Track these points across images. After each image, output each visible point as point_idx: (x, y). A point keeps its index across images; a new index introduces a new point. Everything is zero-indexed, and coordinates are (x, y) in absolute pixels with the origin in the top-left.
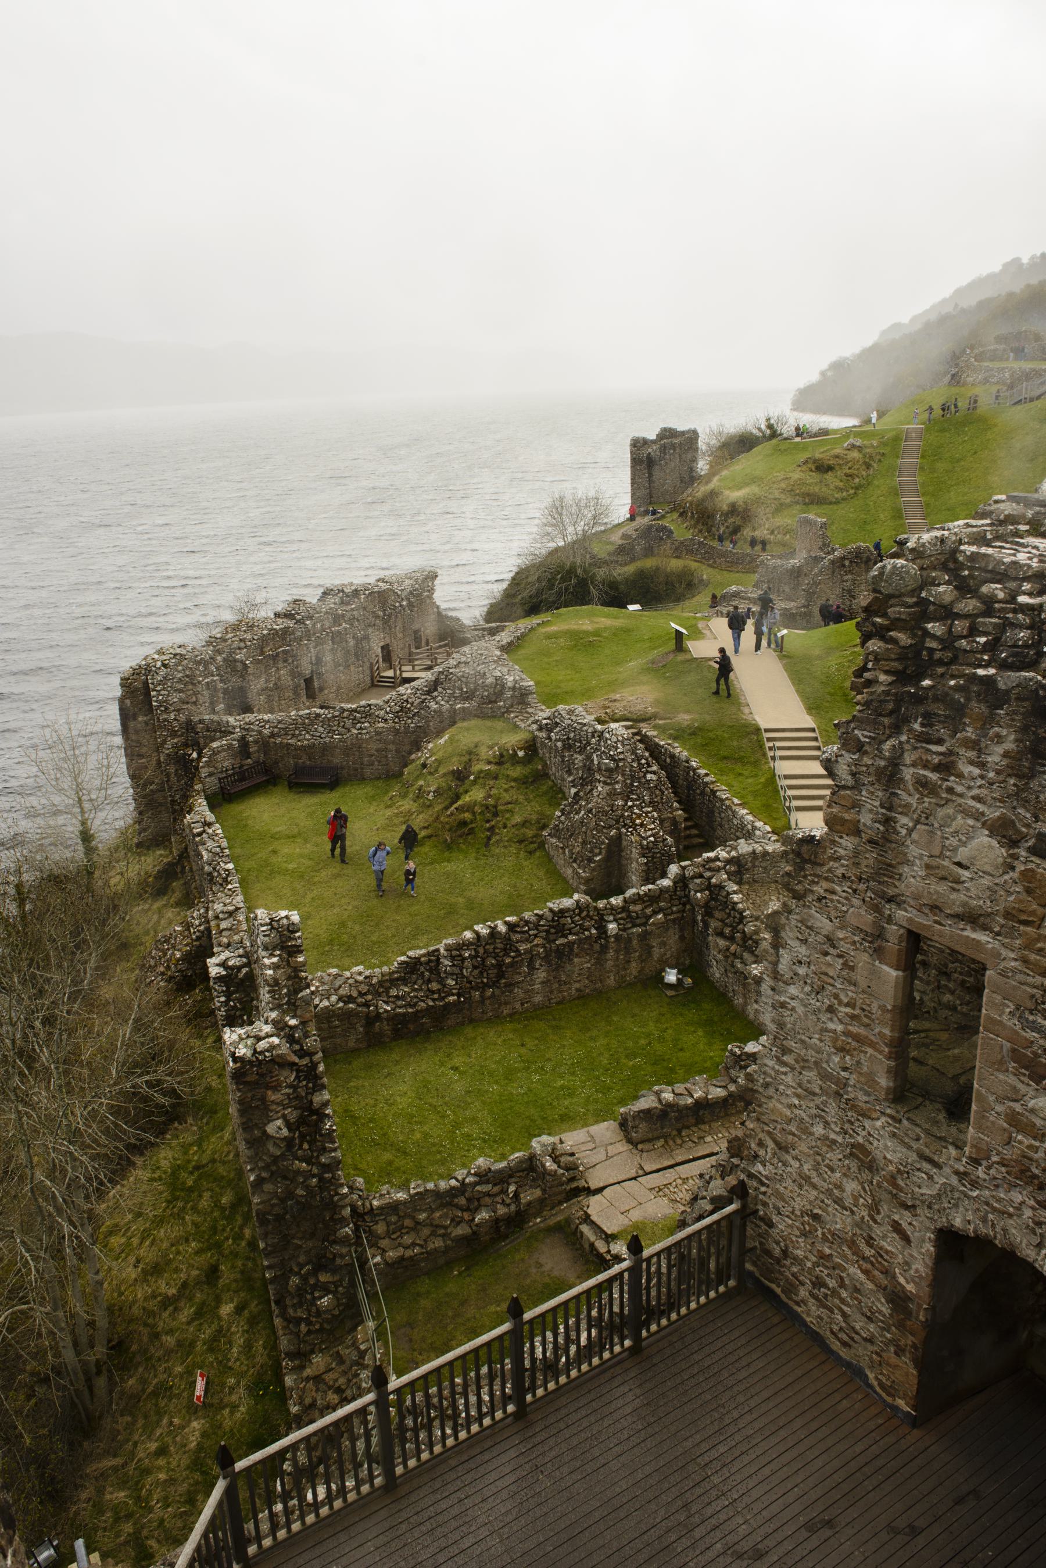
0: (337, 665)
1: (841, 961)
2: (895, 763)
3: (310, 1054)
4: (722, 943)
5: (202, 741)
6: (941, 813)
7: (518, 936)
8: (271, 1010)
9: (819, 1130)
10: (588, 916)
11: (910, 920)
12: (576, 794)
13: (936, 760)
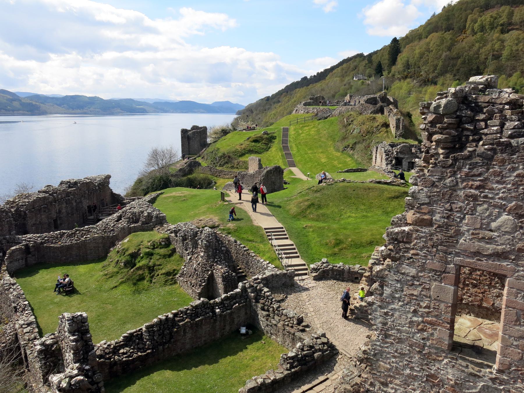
0: (68, 214)
3: (97, 383)
4: (265, 313)
5: (5, 248)
6: (479, 209)
7: (179, 318)
8: (75, 363)
9: (408, 371)
10: (207, 307)
12: (190, 259)
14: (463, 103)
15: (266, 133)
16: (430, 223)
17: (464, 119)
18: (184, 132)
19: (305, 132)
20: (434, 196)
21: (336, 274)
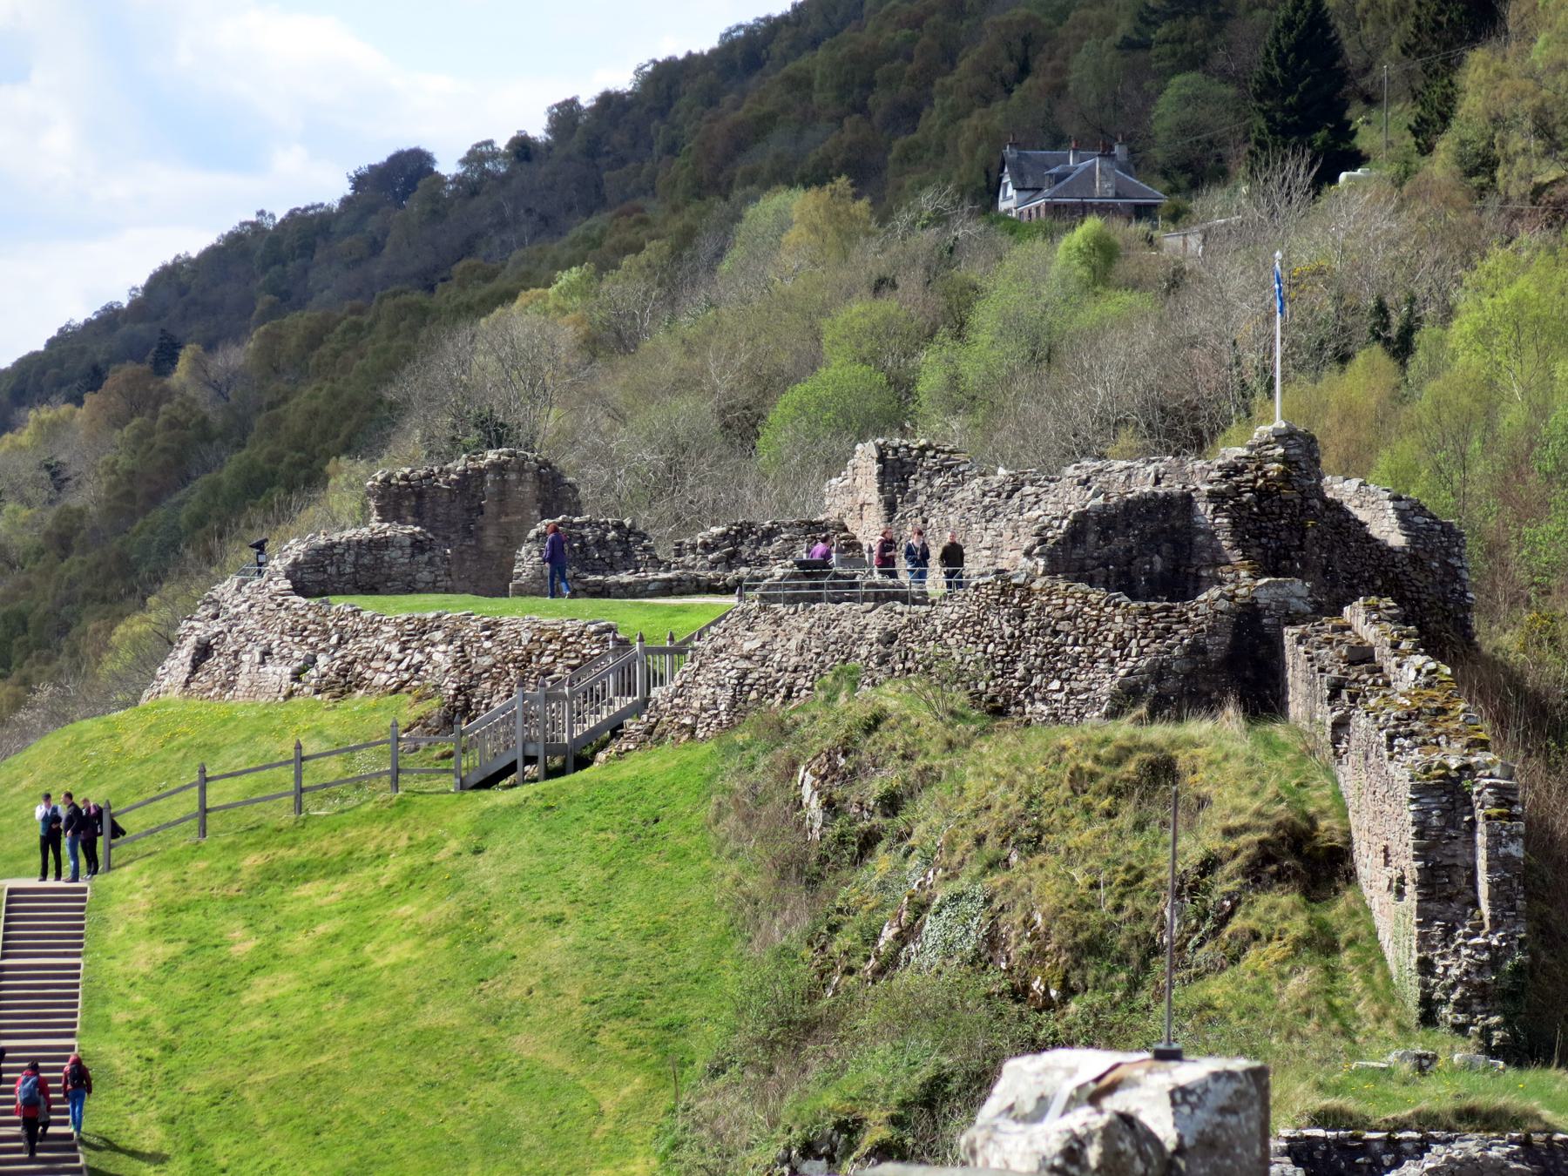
19: (299, 942)
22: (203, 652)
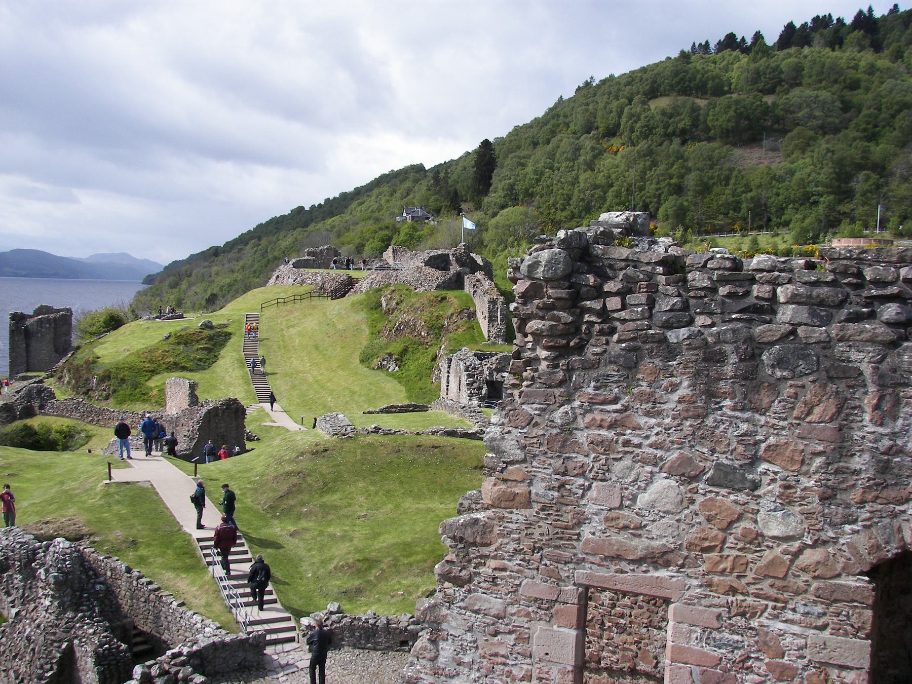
1: (513, 636)
2: (568, 428)
6: (618, 467)
11: (588, 576)
12: (17, 614)
13: (609, 418)
14: (581, 259)
15: (208, 326)
16: (528, 503)
17: (584, 289)
18: (18, 319)
20: (532, 445)
21: (360, 636)
22: (278, 277)
